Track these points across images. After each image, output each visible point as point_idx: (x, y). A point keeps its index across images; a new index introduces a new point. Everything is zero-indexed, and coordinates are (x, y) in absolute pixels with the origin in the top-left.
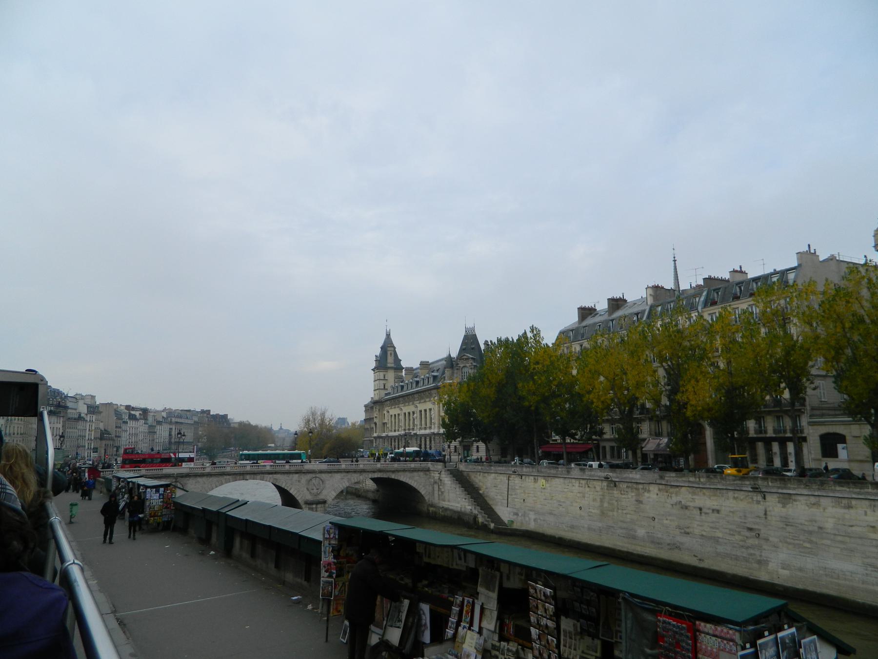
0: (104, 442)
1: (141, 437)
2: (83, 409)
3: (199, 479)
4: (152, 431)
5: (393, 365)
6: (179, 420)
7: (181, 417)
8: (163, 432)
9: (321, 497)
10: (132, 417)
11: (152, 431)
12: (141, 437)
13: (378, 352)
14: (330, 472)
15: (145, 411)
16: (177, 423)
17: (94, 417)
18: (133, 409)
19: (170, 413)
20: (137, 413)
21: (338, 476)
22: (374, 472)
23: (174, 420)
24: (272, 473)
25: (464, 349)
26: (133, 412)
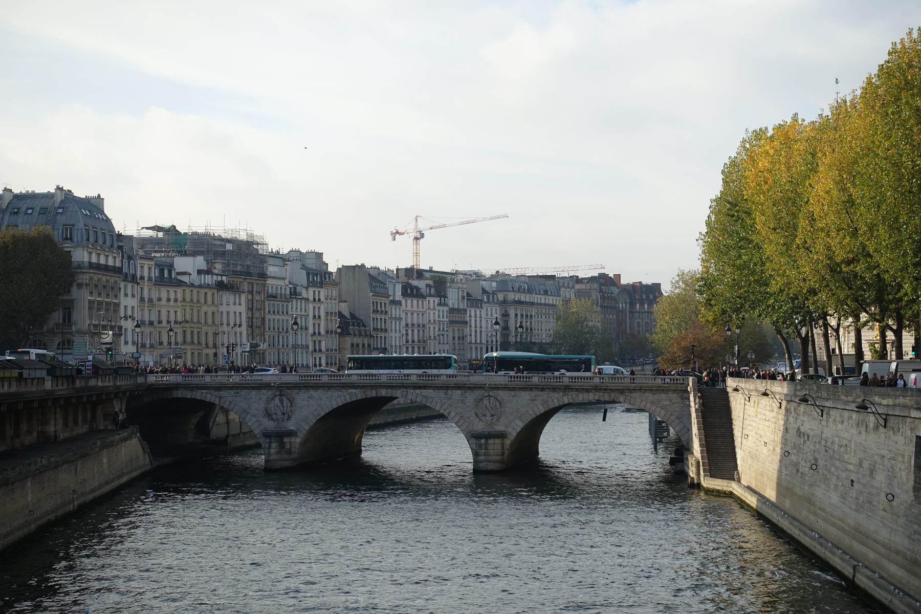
0: (348, 340)
1: (432, 331)
2: (301, 278)
3: (312, 392)
4: (457, 318)
6: (523, 297)
7: (530, 291)
8: (483, 322)
9: (500, 428)
10: (410, 292)
11: (457, 318)
12: (432, 331)
14: (514, 389)
15: (440, 283)
16: (519, 302)
17: (323, 293)
18: (420, 274)
19: (503, 281)
20: (421, 284)
21: (526, 396)
22: (587, 391)
23: (511, 296)
24: (420, 388)
26: (415, 283)
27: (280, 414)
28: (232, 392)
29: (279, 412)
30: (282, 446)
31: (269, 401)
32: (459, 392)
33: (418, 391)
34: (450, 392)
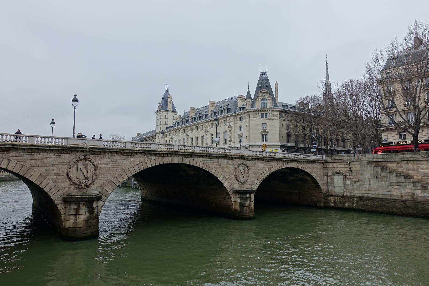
5: (171, 110)
13: (160, 100)
21: (260, 164)
25: (260, 87)
27: (82, 178)
28: (25, 155)
29: (80, 175)
30: (91, 210)
31: (70, 166)
32: (225, 161)
33: (200, 159)
34: (220, 160)
